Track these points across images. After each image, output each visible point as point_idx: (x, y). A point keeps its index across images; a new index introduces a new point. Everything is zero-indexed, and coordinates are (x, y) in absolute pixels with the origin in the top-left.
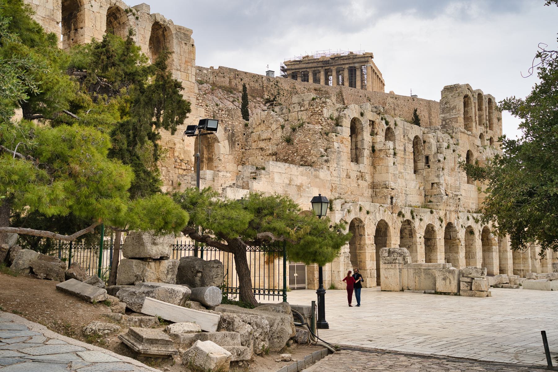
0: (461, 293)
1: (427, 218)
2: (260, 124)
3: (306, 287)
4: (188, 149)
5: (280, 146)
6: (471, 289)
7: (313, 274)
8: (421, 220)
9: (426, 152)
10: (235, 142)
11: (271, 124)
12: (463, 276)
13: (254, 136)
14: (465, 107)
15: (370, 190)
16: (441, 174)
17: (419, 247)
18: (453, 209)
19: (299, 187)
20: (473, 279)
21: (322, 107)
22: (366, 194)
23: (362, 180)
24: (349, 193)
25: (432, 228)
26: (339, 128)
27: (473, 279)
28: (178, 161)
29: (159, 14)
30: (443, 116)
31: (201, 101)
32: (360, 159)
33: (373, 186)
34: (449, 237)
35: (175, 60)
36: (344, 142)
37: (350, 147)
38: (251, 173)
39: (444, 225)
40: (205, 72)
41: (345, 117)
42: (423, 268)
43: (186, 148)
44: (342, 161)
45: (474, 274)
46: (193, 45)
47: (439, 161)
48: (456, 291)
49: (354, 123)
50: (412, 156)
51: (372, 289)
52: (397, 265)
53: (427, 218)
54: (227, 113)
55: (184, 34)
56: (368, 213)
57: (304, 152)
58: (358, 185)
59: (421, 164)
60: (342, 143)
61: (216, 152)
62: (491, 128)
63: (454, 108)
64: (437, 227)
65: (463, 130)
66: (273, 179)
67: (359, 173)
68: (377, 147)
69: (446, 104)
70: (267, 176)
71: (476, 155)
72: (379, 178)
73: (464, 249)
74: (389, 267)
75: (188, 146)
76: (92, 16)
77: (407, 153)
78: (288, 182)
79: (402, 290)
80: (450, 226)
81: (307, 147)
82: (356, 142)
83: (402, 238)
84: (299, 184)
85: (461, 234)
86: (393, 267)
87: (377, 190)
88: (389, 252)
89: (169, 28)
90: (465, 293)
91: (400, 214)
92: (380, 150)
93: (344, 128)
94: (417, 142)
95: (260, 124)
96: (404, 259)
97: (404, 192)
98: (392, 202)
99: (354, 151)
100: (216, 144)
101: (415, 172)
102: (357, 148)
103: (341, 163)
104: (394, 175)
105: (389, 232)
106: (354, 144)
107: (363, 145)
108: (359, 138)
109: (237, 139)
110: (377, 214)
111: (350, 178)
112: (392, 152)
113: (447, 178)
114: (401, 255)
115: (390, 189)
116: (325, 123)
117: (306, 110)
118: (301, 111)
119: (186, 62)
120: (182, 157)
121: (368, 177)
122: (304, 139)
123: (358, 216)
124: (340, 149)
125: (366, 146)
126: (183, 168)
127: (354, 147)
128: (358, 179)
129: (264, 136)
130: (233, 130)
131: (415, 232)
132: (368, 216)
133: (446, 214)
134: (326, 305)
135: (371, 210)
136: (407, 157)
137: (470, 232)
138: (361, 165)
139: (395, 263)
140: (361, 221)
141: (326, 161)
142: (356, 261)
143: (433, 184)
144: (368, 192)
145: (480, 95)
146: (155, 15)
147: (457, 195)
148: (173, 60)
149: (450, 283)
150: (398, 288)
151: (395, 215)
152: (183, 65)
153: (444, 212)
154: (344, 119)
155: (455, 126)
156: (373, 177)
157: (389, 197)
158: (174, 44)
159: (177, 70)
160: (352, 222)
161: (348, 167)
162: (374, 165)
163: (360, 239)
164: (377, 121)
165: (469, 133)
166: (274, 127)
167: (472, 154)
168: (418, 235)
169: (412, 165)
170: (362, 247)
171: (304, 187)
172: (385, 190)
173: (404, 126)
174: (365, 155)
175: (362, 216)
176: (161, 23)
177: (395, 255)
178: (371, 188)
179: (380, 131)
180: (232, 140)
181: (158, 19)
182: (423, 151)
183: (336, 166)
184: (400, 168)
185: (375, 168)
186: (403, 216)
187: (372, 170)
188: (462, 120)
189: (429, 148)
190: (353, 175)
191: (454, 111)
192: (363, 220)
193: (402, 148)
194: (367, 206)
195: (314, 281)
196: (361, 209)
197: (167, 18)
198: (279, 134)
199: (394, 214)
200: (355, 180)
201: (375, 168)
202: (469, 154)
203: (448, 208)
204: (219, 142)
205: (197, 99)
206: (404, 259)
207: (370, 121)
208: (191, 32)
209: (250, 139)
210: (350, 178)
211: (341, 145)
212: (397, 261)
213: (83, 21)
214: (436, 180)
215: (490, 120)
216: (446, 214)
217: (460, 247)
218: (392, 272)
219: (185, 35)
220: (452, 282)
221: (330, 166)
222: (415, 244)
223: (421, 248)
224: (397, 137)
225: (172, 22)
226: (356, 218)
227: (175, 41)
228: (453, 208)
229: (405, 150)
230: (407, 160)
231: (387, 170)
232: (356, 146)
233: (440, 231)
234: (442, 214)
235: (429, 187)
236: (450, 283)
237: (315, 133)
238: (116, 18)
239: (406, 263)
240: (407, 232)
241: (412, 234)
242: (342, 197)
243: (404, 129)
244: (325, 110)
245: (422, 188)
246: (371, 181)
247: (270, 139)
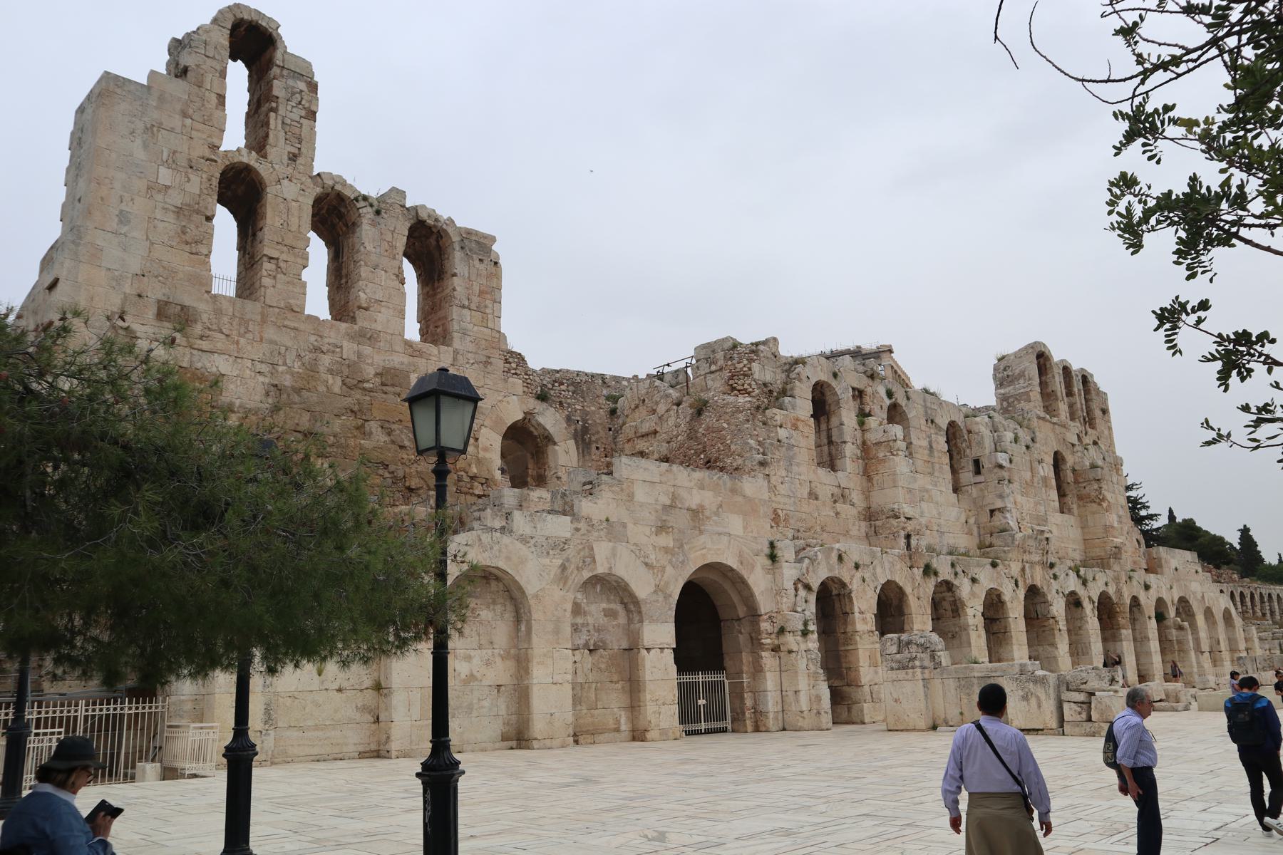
0: (1067, 728)
1: (987, 579)
2: (637, 407)
3: (729, 727)
4: (488, 455)
5: (673, 444)
6: (1089, 719)
7: (742, 698)
8: (974, 580)
9: (974, 452)
10: (590, 443)
11: (657, 403)
12: (1068, 690)
13: (628, 430)
14: (1040, 374)
15: (863, 524)
16: (1007, 491)
17: (973, 635)
19: (697, 514)
20: (1092, 694)
21: (751, 361)
22: (854, 532)
23: (844, 503)
24: (818, 528)
25: (999, 596)
26: (787, 399)
27: (1092, 694)
28: (466, 479)
29: (423, 207)
30: (1002, 391)
31: (514, 365)
32: (838, 462)
33: (870, 515)
34: (1033, 615)
35: (458, 289)
36: (801, 428)
37: (813, 436)
38: (585, 484)
39: (1021, 593)
40: (625, 383)
41: (800, 380)
42: (976, 674)
43: (481, 454)
44: (798, 465)
45: (1093, 684)
46: (496, 263)
47: (1001, 467)
48: (1054, 724)
49: (823, 394)
50: (946, 459)
51: (876, 727)
52: (918, 671)
53: (987, 579)
54: (571, 388)
55: (478, 243)
56: (857, 567)
57: (719, 450)
58: (837, 514)
59: (967, 476)
60: (796, 429)
61: (552, 464)
62: (1093, 426)
63: (1022, 375)
64: (1007, 597)
65: (1042, 414)
66: (631, 496)
67: (836, 491)
68: (872, 437)
69: (1005, 370)
70: (616, 489)
71: (1070, 460)
72: (880, 499)
73: (1066, 636)
74: (900, 677)
75: (486, 449)
76: (282, 206)
77: (936, 454)
78: (668, 502)
79: (934, 728)
80: (1033, 593)
81: (722, 440)
82: (829, 430)
83: (936, 618)
84: (694, 507)
85: (1058, 608)
86: (910, 677)
87: (878, 523)
88: (902, 646)
89: (445, 231)
90: (1077, 730)
91: (928, 571)
92: (879, 444)
93: (798, 401)
94: (954, 434)
95: (637, 407)
96: (933, 657)
97: (936, 528)
98: (908, 546)
99: (826, 448)
100: (550, 447)
101: (956, 490)
102: (830, 442)
103: (795, 468)
104: (910, 491)
105: (909, 606)
106: (824, 435)
107: (841, 433)
108: (834, 421)
109: (593, 439)
110: (879, 570)
111: (817, 499)
112: (902, 445)
113: (1019, 498)
114: (924, 648)
115: (903, 519)
116: (757, 391)
117: (721, 370)
118: (712, 372)
119: (481, 293)
120: (474, 470)
121: (856, 497)
122: (717, 425)
123: (836, 573)
124: (792, 442)
125: (848, 438)
126: (477, 492)
127: (826, 441)
128: (835, 502)
129: (645, 428)
130: (585, 421)
131: (963, 604)
132: (858, 574)
133: (1023, 570)
134: (462, 831)
135: (866, 559)
136: (936, 460)
137: (1074, 602)
138: (840, 474)
139: (913, 667)
140: (843, 585)
141: (763, 464)
142: (840, 667)
143: (992, 511)
144: (860, 528)
145: (1066, 370)
146: (415, 208)
147: (1043, 532)
148: (454, 290)
149: (1039, 707)
150: (922, 724)
151: (918, 572)
152: (475, 299)
153: (1020, 565)
154: (797, 383)
155: (1026, 409)
156: (867, 498)
157: (902, 533)
158: (457, 261)
159: (463, 307)
160: (823, 584)
161: (812, 477)
162: (867, 474)
163: (845, 623)
164: (869, 390)
165: (1055, 420)
166: (661, 408)
167: (1063, 459)
168: (970, 612)
169: (949, 476)
170: (849, 639)
171: (707, 513)
172: (894, 522)
174: (848, 453)
175: (845, 574)
176: (431, 222)
177: (913, 648)
178: (865, 520)
179: (876, 409)
180: (583, 440)
181: (423, 215)
183: (784, 473)
184: (922, 481)
185: (870, 479)
186: (936, 574)
187: (865, 484)
188: (1039, 397)
189: (980, 444)
190: (825, 492)
191: (1021, 381)
192: (846, 580)
193: (925, 443)
194: (856, 550)
195: (744, 713)
196: (840, 558)
197: (443, 212)
198: (671, 422)
199: (915, 570)
200: (829, 501)
201: (870, 479)
202: (1058, 460)
203: (1026, 557)
204: (555, 444)
205: (507, 362)
206: (933, 657)
207: (854, 389)
208: (493, 239)
209: (621, 438)
210: (817, 499)
211: (795, 433)
212: (917, 663)
213: (263, 217)
214: (999, 504)
215: (1089, 411)
216: (1023, 570)
217: (1056, 632)
218: (908, 687)
219: (480, 246)
220: (1044, 704)
221: (772, 473)
222: (965, 628)
223: (979, 636)
224: (913, 423)
225: (453, 222)
226: (831, 579)
227: (458, 255)
228: (1036, 558)
230: (937, 466)
231: (894, 481)
232: (829, 437)
233: (1015, 603)
234: (1015, 568)
235: (985, 517)
236: (1039, 707)
237: (738, 410)
238: (341, 216)
239: (938, 665)
240: (945, 606)
241: (957, 611)
242: (800, 535)
243: (926, 407)
244: (756, 367)
245: (972, 521)
246: (864, 505)
247: (655, 432)
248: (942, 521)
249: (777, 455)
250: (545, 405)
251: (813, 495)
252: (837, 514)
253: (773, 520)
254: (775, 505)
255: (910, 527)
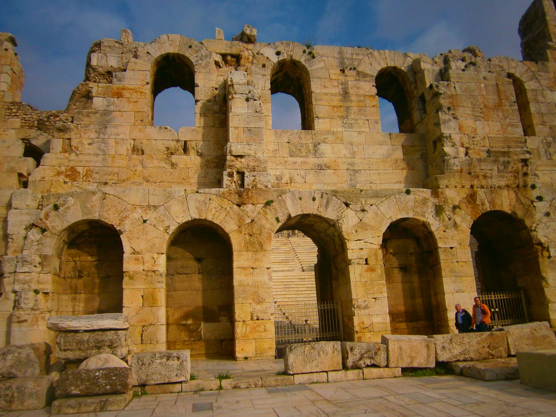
18: (503, 183)
44: (116, 126)
58: (173, 165)
77: (353, 98)
97: (345, 167)
111: (143, 153)
124: (112, 108)
161: (136, 134)
173: (340, 53)
182: (415, 91)
183: (94, 135)
229: (345, 94)
248: (357, 160)
249: (86, 120)
250: (39, 132)
251: (138, 150)
252: (173, 165)
253: (67, 176)
254: (72, 164)
255: (239, 164)
